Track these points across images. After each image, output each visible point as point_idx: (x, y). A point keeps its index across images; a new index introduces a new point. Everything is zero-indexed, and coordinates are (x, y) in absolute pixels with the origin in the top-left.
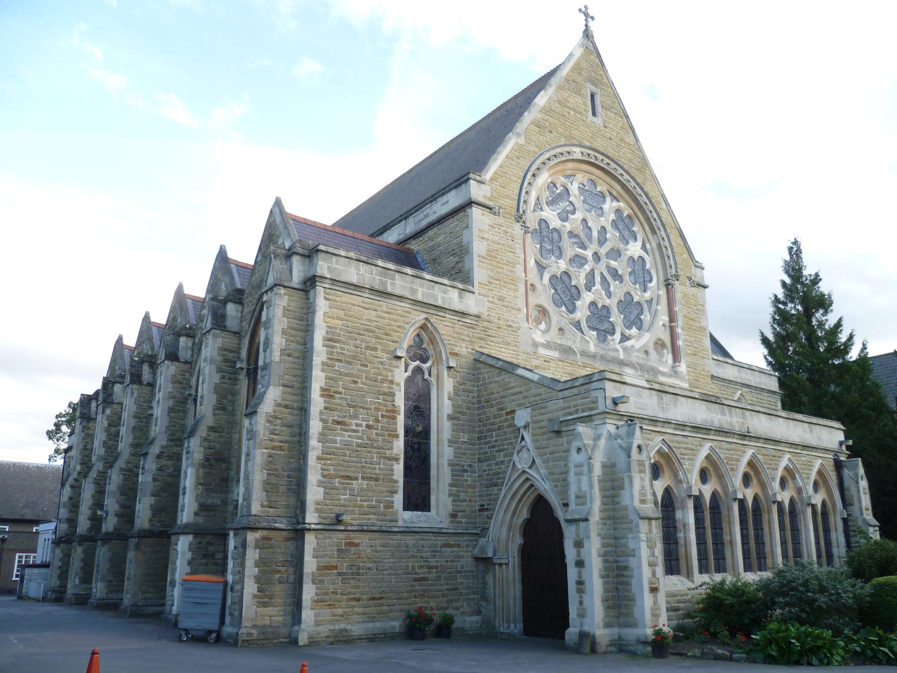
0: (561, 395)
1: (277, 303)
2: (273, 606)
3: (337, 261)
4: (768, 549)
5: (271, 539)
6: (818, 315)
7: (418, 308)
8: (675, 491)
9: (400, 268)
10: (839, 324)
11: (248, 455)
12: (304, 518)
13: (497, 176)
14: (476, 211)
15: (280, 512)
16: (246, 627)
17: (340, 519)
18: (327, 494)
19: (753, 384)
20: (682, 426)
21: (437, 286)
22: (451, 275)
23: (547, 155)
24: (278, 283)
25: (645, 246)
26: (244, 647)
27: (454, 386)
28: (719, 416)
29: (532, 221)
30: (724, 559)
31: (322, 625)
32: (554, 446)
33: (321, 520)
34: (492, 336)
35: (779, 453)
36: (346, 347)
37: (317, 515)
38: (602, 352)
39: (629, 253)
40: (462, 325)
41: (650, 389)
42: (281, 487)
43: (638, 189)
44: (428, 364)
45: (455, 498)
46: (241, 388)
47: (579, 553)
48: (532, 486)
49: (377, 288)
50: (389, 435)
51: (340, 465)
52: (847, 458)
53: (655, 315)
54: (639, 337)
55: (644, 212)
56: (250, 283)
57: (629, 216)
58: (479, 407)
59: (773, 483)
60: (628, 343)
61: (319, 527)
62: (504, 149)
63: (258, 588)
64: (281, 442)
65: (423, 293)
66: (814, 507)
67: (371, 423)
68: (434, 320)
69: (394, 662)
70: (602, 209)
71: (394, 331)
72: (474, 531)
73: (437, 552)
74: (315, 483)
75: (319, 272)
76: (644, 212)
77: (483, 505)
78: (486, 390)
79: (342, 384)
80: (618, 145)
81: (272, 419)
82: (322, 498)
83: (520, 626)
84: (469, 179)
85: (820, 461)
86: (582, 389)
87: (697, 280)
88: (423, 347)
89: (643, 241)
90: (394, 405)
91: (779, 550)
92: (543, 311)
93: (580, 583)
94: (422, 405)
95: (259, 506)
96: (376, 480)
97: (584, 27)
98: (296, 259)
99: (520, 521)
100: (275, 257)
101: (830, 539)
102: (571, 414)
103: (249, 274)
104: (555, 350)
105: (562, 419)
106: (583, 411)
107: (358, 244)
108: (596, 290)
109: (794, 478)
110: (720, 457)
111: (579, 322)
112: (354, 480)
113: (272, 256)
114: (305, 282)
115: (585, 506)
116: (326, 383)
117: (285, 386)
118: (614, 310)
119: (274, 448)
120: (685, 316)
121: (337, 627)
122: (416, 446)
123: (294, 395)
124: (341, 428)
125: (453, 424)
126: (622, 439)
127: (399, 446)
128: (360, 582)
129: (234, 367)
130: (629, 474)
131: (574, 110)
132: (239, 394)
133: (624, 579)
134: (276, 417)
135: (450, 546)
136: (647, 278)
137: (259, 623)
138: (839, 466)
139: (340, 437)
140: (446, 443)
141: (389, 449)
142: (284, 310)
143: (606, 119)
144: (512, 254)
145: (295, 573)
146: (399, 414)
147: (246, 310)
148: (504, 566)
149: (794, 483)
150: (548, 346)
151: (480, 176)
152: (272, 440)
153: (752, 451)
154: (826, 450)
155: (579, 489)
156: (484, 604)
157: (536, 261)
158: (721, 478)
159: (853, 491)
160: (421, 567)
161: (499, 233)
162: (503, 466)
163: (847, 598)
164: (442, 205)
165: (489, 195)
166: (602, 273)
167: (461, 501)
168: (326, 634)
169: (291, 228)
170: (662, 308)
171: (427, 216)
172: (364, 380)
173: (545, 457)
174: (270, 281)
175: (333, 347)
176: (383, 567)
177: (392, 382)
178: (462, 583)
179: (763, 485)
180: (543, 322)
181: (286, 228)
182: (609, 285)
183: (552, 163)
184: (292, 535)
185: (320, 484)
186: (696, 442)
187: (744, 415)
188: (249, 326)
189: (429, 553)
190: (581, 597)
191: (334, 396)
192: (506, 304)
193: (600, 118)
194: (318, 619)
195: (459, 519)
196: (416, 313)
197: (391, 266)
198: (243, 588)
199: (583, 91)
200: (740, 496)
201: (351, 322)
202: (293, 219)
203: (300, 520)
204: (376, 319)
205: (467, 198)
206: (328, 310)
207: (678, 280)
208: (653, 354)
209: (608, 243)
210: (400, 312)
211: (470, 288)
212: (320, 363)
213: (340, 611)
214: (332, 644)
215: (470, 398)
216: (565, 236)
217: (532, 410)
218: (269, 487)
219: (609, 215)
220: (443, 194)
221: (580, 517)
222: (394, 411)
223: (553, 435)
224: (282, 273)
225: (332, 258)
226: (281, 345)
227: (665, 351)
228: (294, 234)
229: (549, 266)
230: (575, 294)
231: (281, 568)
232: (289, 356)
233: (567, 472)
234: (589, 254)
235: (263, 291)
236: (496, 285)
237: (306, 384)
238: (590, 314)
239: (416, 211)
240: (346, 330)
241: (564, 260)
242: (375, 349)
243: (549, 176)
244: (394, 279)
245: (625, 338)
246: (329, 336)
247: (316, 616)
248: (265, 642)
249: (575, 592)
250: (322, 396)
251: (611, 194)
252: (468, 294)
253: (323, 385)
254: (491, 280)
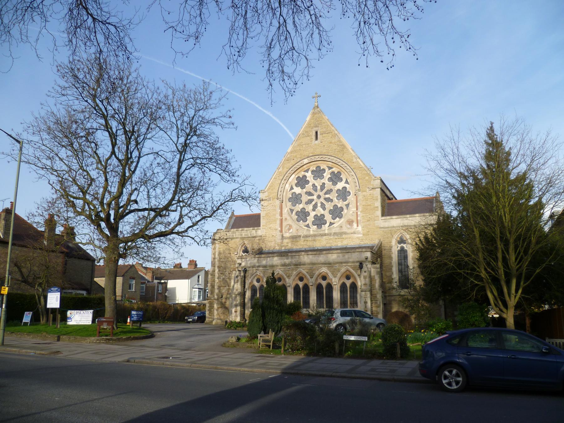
39: (336, 189)
43: (338, 160)
227: (354, 223)
234: (315, 197)
245: (331, 224)
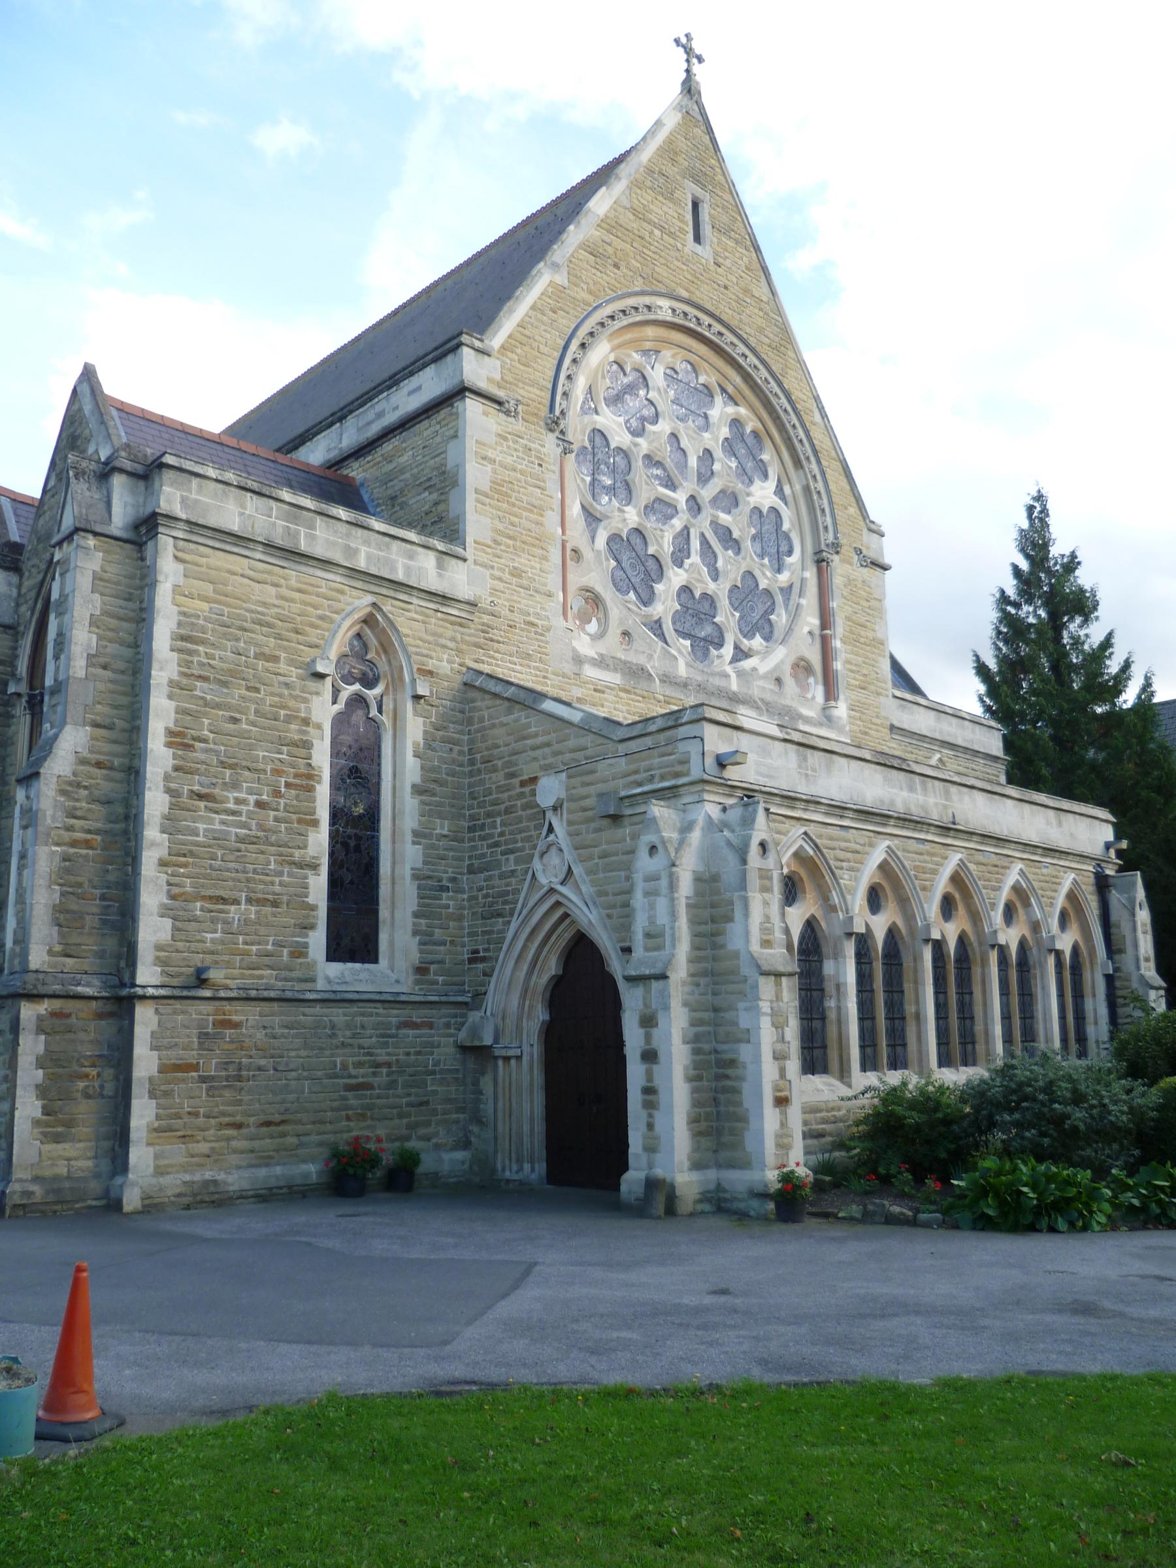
0: (622, 748)
1: (79, 564)
2: (72, 1140)
3: (200, 487)
4: (979, 1028)
5: (68, 1016)
6: (1072, 627)
7: (359, 584)
8: (823, 924)
9: (324, 507)
10: (1107, 643)
11: (23, 856)
12: (133, 975)
13: (513, 342)
14: (472, 407)
15: (86, 964)
16: (21, 1180)
17: (204, 976)
18: (179, 930)
19: (960, 742)
20: (838, 809)
21: (396, 545)
22: (424, 526)
23: (608, 310)
24: (82, 526)
25: (782, 490)
26: (17, 1217)
27: (425, 732)
28: (905, 794)
29: (577, 428)
30: (904, 1045)
31: (168, 1173)
32: (608, 843)
33: (167, 980)
34: (499, 642)
35: (1004, 862)
36: (217, 653)
37: (159, 969)
38: (699, 678)
39: (752, 501)
40: (442, 620)
41: (785, 740)
42: (88, 918)
44: (378, 690)
45: (426, 939)
46: (17, 733)
47: (648, 1038)
48: (566, 915)
49: (279, 542)
50: (300, 821)
51: (205, 877)
52: (1118, 871)
53: (795, 615)
54: (766, 653)
55: (781, 428)
56: (34, 531)
57: (755, 433)
58: (471, 771)
59: (992, 913)
60: (747, 664)
61: (162, 992)
62: (528, 292)
63: (44, 1107)
64: (89, 832)
65: (369, 557)
66: (1058, 954)
67: (264, 797)
68: (389, 608)
69: (301, 1242)
70: (706, 416)
71: (312, 626)
72: (460, 999)
73: (390, 1036)
74: (156, 910)
75: (164, 507)
76: (781, 428)
77: (477, 952)
78: (484, 739)
79: (210, 724)
80: (739, 301)
81: (69, 788)
82: (169, 938)
83: (541, 1168)
84: (459, 345)
85: (1073, 875)
86: (662, 737)
87: (872, 554)
88: (368, 657)
89: (779, 481)
90: (310, 765)
91: (998, 1030)
92: (594, 600)
93: (649, 1091)
94: (363, 766)
95: (45, 954)
96: (275, 904)
97: (684, 75)
98: (118, 481)
99: (545, 978)
100: (76, 476)
101: (1083, 1010)
102: (640, 784)
103: (32, 516)
104: (615, 670)
105: (623, 793)
106: (663, 778)
107: (247, 463)
108: (691, 565)
109: (1027, 904)
110: (904, 867)
111: (659, 622)
112: (232, 904)
113: (71, 473)
114: (136, 527)
115: (662, 952)
116: (176, 721)
117: (96, 725)
118: (724, 603)
119: (74, 843)
120: (848, 619)
121: (197, 1177)
122: (352, 843)
123: (115, 742)
124: (206, 807)
125: (423, 803)
126: (733, 831)
127: (319, 841)
128: (243, 1093)
129: (5, 692)
130: (743, 893)
131: (662, 229)
132: (13, 744)
133: (729, 1083)
134: (79, 785)
135: (415, 1026)
136: (784, 548)
137: (48, 1173)
138: (1102, 884)
139: (205, 824)
140: (409, 838)
141: (299, 848)
142: (94, 579)
143: (719, 249)
144: (539, 491)
145: (117, 1078)
146: (319, 782)
147: (27, 584)
148: (513, 1062)
149: (1027, 914)
150: (601, 662)
151: (481, 340)
152: (70, 829)
153: (959, 856)
154: (1082, 857)
155: (652, 920)
156: (475, 1129)
157: (583, 507)
158: (904, 903)
159: (1126, 928)
160: (359, 1065)
161: (516, 450)
162: (513, 880)
163: (1119, 1114)
164: (410, 393)
165: (498, 377)
166: (702, 535)
167: (435, 944)
168: (178, 1191)
169: (111, 423)
170: (809, 602)
171: (380, 415)
172: (252, 717)
173: (592, 863)
174: (68, 523)
175: (190, 653)
176: (287, 1065)
177: (306, 722)
178: (435, 1092)
179: (975, 917)
180: (594, 619)
181: (103, 423)
182: (715, 557)
183: (617, 324)
184: (109, 1007)
185: (165, 912)
186: (862, 838)
187: (947, 793)
188: (32, 614)
189: (374, 1039)
190: (650, 1116)
191: (192, 746)
192: (525, 582)
193: (708, 247)
194: (162, 1162)
195: (432, 977)
196: (355, 593)
197: (307, 502)
198: (13, 1109)
199: (678, 194)
200: (936, 935)
201: (229, 606)
202: (118, 409)
203: (126, 980)
204: (276, 602)
205: (456, 381)
206: (181, 581)
207: (837, 553)
208: (790, 683)
209: (715, 480)
210: (323, 590)
211: (459, 550)
212: (165, 681)
213: (203, 1147)
214: (188, 1207)
215: (455, 755)
216: (638, 464)
217: (569, 777)
218: (64, 918)
219: (719, 428)
220: (412, 374)
221: (653, 971)
222: (310, 777)
223: (606, 822)
224: (90, 506)
225: (190, 481)
226: (89, 646)
227: (811, 680)
228: (119, 436)
229: (607, 517)
230: (653, 570)
231: (88, 1070)
232: (105, 667)
233: (629, 891)
234: (680, 497)
235: (54, 541)
236: (508, 546)
237: (138, 722)
238: (679, 607)
239: (361, 406)
240: (217, 620)
241: (635, 507)
242: (275, 659)
243: (612, 350)
244: (312, 527)
245: (741, 654)
246: (182, 632)
247: (157, 1157)
248: (58, 1207)
249: (639, 1106)
250: (169, 745)
251: (723, 390)
252: (454, 561)
253: (171, 725)
254: (499, 538)
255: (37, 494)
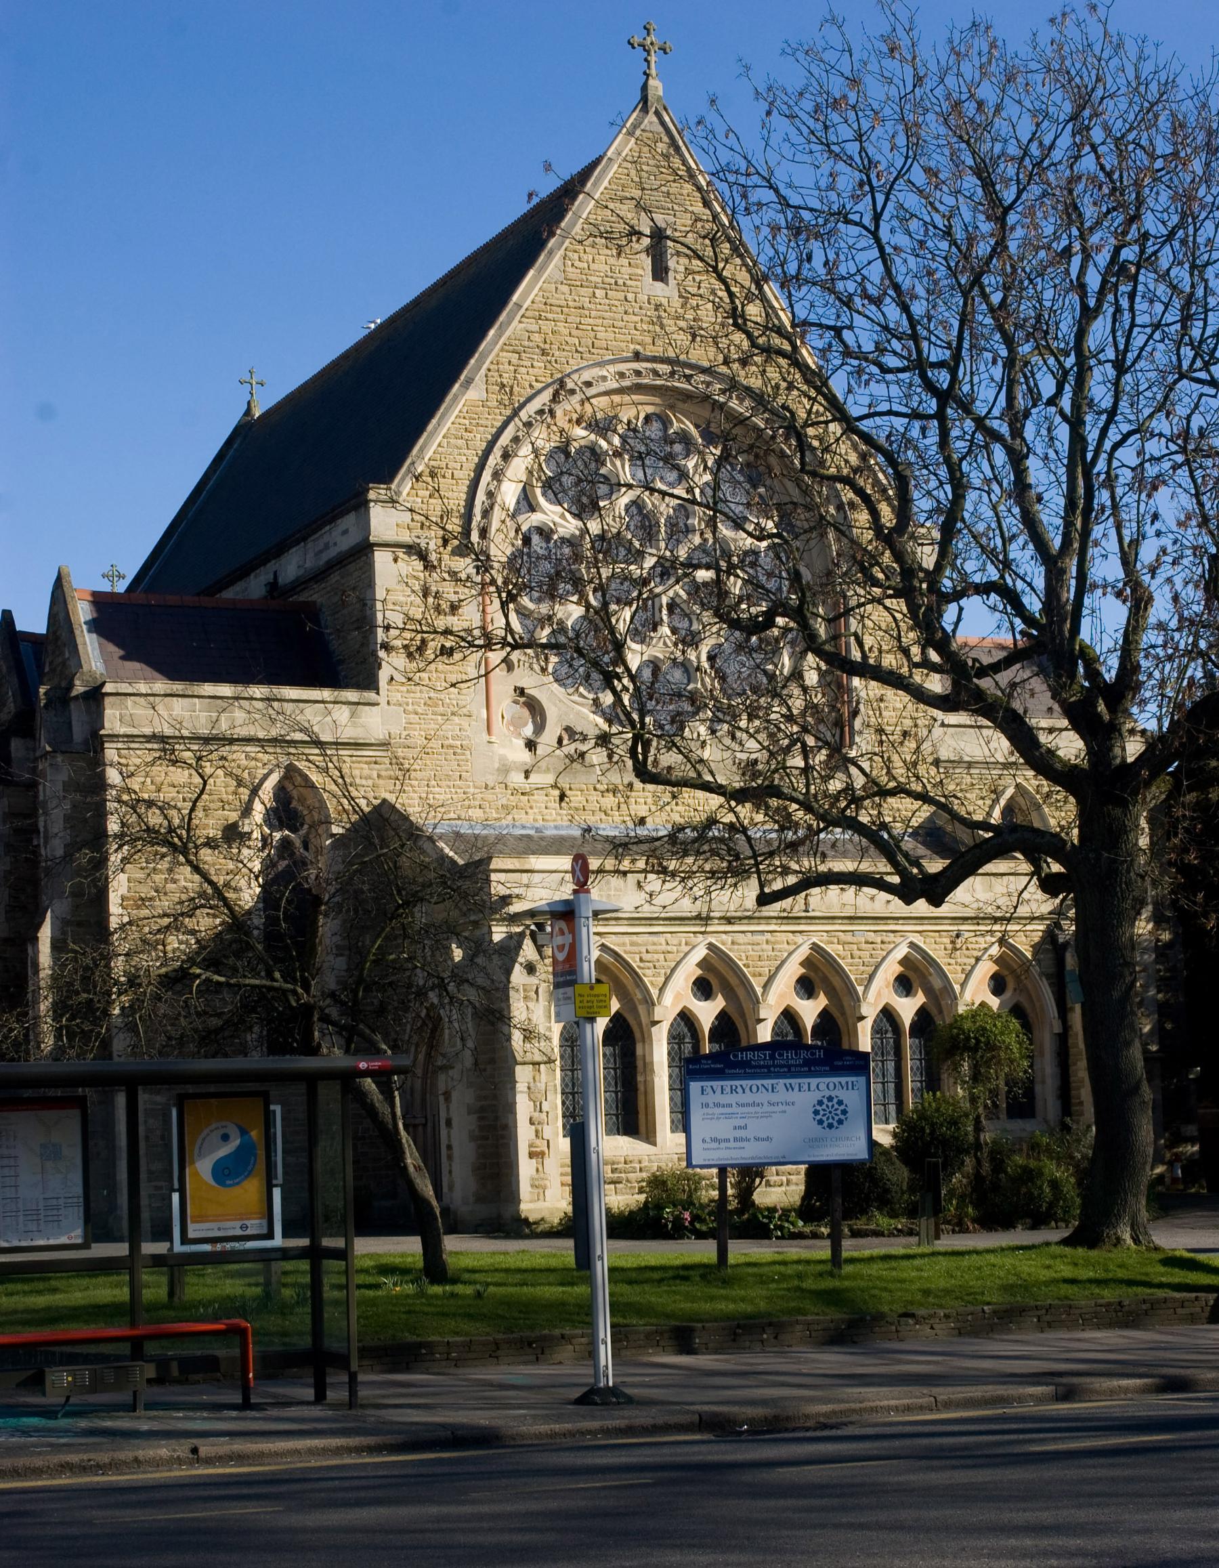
116: (129, 888)
148: (420, 1129)
197: (226, 690)
255: (44, 632)
